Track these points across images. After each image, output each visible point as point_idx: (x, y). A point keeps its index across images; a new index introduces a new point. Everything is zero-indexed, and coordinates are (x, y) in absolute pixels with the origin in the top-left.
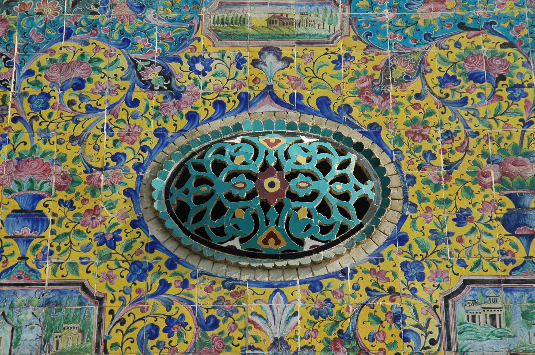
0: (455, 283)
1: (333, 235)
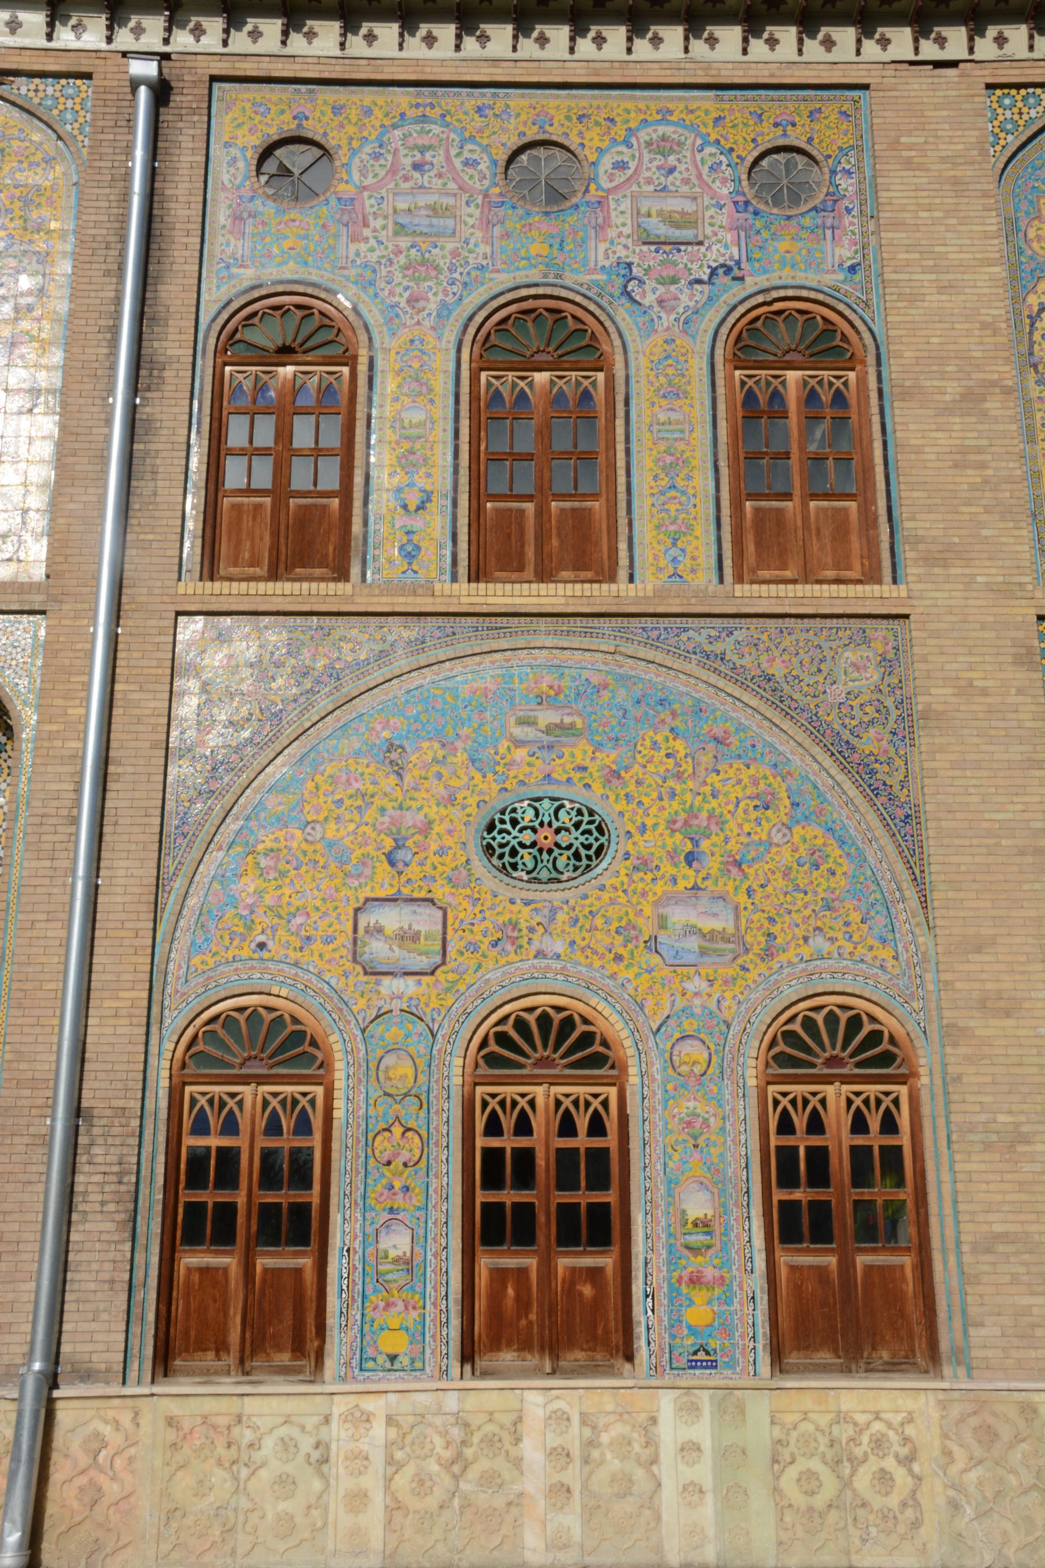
1: (579, 872)
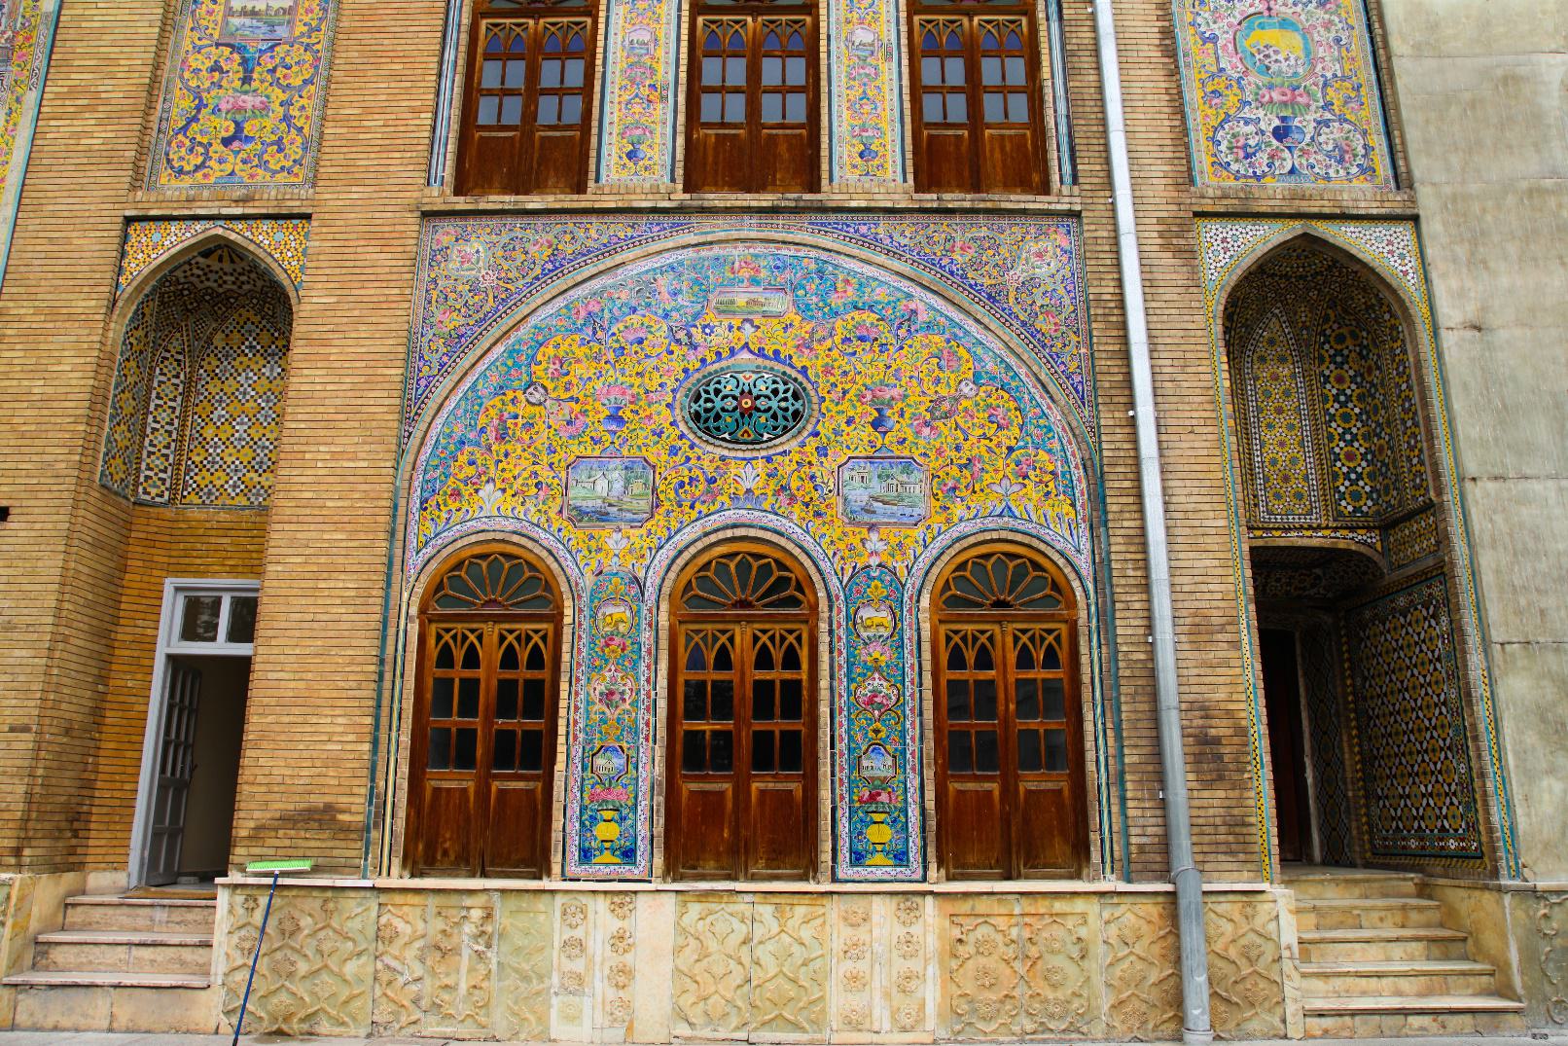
0: (844, 459)
1: (779, 431)
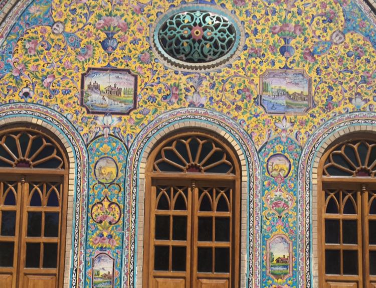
1: (216, 56)
